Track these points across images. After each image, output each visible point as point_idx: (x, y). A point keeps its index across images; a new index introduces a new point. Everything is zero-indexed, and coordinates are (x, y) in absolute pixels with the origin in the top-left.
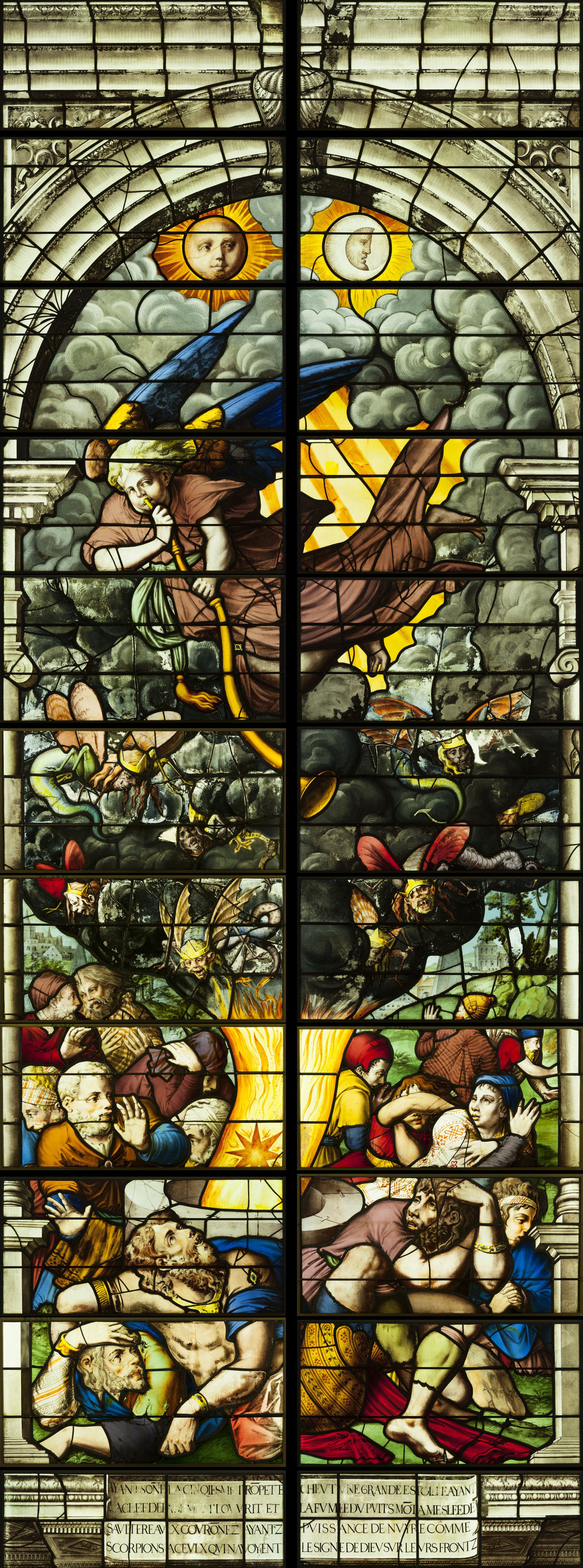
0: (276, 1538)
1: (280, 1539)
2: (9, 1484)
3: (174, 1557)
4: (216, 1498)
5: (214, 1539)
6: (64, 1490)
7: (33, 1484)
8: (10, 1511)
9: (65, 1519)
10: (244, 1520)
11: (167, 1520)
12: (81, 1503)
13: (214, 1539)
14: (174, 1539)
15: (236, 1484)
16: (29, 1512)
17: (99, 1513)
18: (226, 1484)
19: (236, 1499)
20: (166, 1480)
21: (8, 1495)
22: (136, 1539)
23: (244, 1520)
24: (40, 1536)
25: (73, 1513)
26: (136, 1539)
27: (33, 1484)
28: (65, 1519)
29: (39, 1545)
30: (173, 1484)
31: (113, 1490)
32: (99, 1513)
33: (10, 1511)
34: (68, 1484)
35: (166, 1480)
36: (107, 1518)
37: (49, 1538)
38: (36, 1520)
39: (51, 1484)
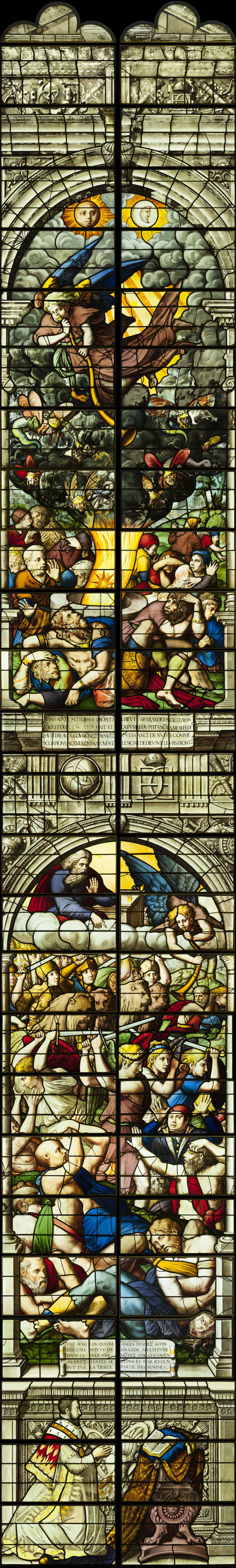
0: (112, 739)
1: (113, 740)
2: (4, 717)
3: (70, 747)
4: (87, 723)
5: (87, 740)
6: (26, 719)
7: (13, 717)
8: (4, 728)
9: (26, 732)
10: (99, 732)
11: (68, 732)
12: (32, 725)
13: (87, 740)
14: (70, 740)
15: (96, 717)
16: (12, 729)
17: (40, 729)
18: (91, 717)
19: (95, 723)
20: (67, 715)
21: (3, 722)
22: (55, 739)
23: (99, 732)
24: (16, 738)
25: (30, 729)
26: (55, 739)
27: (13, 717)
28: (26, 732)
29: (16, 742)
30: (70, 717)
31: (46, 719)
32: (40, 729)
33: (4, 728)
34: (27, 717)
35: (67, 715)
36: (43, 731)
37: (20, 739)
38: (15, 732)
39: (21, 717)
